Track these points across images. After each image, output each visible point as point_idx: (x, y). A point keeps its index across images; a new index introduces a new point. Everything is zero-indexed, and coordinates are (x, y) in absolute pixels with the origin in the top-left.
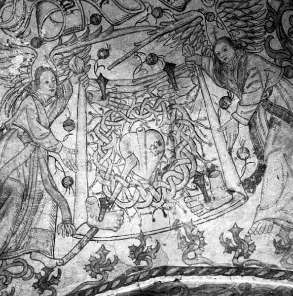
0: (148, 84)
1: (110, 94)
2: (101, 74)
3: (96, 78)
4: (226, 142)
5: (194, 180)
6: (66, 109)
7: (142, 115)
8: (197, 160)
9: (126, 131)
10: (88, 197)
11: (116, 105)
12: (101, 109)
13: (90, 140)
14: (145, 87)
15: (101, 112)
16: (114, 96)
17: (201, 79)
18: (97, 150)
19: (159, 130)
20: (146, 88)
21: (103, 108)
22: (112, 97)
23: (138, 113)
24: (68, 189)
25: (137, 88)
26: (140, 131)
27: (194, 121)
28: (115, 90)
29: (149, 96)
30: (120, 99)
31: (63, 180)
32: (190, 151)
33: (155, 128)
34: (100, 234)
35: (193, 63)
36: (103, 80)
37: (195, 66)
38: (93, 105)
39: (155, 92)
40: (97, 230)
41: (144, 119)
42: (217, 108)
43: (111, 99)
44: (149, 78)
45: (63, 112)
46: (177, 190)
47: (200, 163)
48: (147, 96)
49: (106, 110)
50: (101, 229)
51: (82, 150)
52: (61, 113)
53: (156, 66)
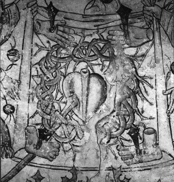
0: (99, 23)
1: (59, 27)
2: (51, 3)
3: (46, 6)
4: (168, 106)
5: (129, 132)
6: (11, 37)
7: (89, 56)
8: (136, 114)
9: (70, 70)
10: (28, 126)
11: (63, 39)
12: (48, 42)
13: (34, 73)
14: (95, 26)
15: (47, 45)
16: (62, 30)
17: (157, 34)
18: (40, 84)
19: (103, 76)
20: (96, 28)
21: (50, 41)
22: (60, 31)
23: (85, 54)
24: (9, 116)
25: (87, 25)
26: (85, 73)
27: (140, 77)
28: (64, 24)
29: (98, 38)
30: (69, 34)
31: (4, 107)
32: (131, 104)
33: (101, 73)
34: (38, 161)
35: (152, 15)
36: (53, 10)
37: (153, 19)
38: (40, 36)
39: (105, 35)
40: (34, 156)
41: (89, 61)
42: (167, 70)
43: (59, 33)
44: (101, 18)
45: (7, 40)
46: (112, 137)
47: (137, 118)
48: (96, 36)
49: (53, 43)
50: (38, 156)
51: (25, 80)
52: (6, 41)
53: (109, 6)
